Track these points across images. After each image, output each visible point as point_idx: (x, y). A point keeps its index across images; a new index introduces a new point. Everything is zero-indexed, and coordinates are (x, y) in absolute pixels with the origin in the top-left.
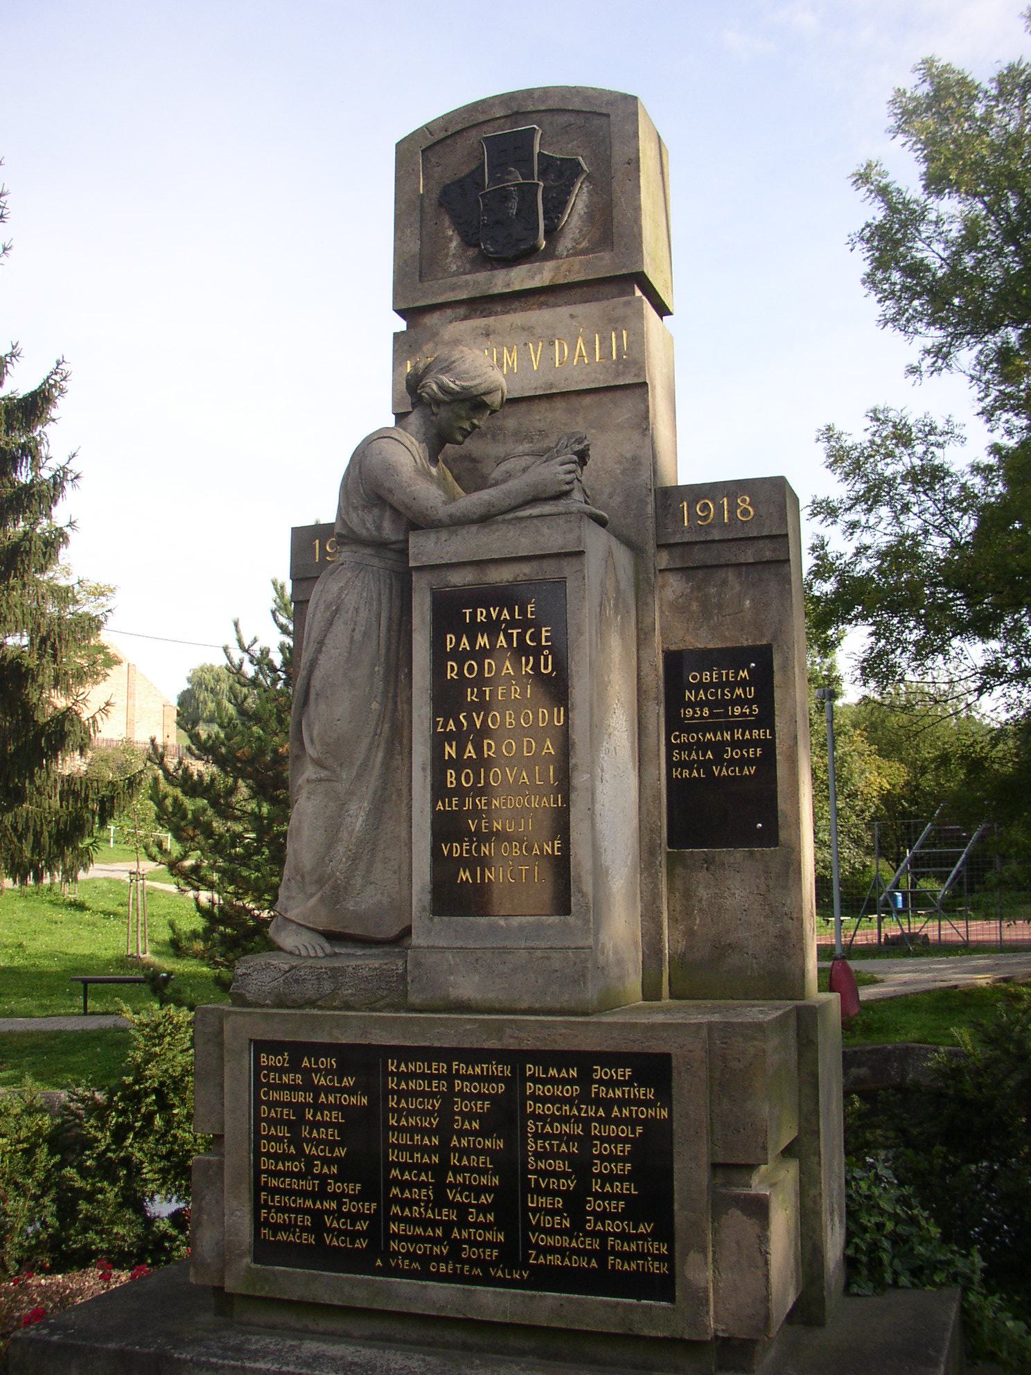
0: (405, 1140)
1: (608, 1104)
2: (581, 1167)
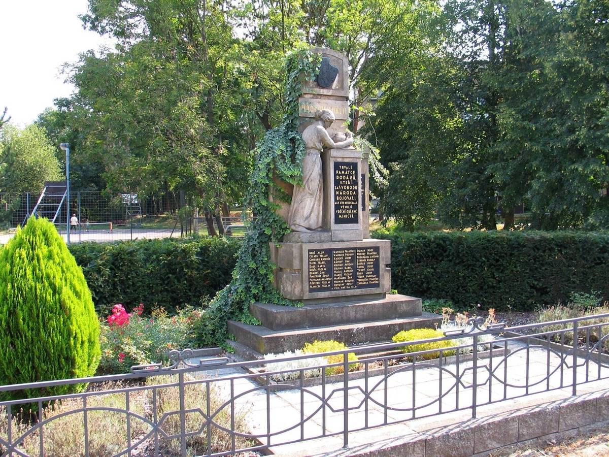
0: (337, 265)
1: (369, 256)
2: (366, 266)
